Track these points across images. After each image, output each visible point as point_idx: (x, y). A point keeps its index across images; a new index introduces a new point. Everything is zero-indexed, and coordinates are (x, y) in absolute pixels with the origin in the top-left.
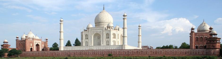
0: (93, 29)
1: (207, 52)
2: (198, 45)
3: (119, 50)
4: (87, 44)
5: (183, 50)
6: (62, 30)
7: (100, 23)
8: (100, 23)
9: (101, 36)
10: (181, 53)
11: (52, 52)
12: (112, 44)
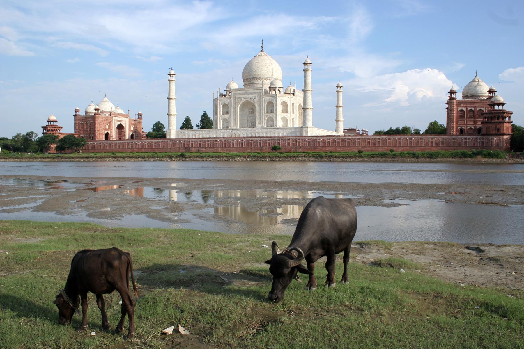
0: (238, 92)
1: (483, 142)
2: (463, 127)
3: (295, 138)
4: (226, 125)
5: (432, 137)
6: (173, 95)
7: (254, 78)
8: (254, 78)
9: (257, 107)
10: (427, 143)
11: (152, 142)
12: (280, 123)
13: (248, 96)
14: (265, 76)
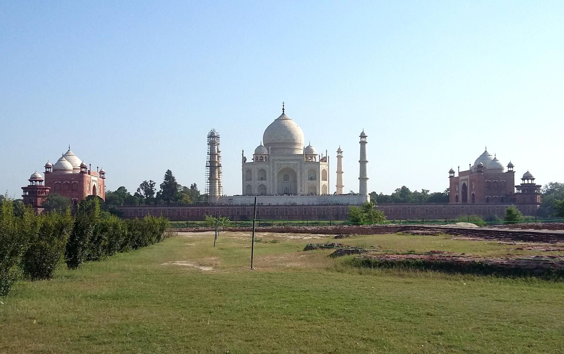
9: (299, 174)
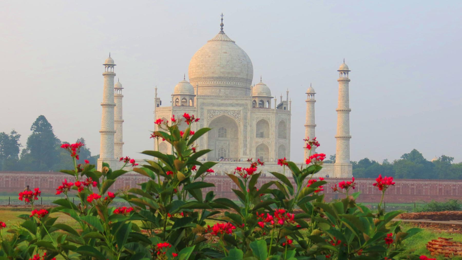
13: (226, 108)
14: (239, 76)
